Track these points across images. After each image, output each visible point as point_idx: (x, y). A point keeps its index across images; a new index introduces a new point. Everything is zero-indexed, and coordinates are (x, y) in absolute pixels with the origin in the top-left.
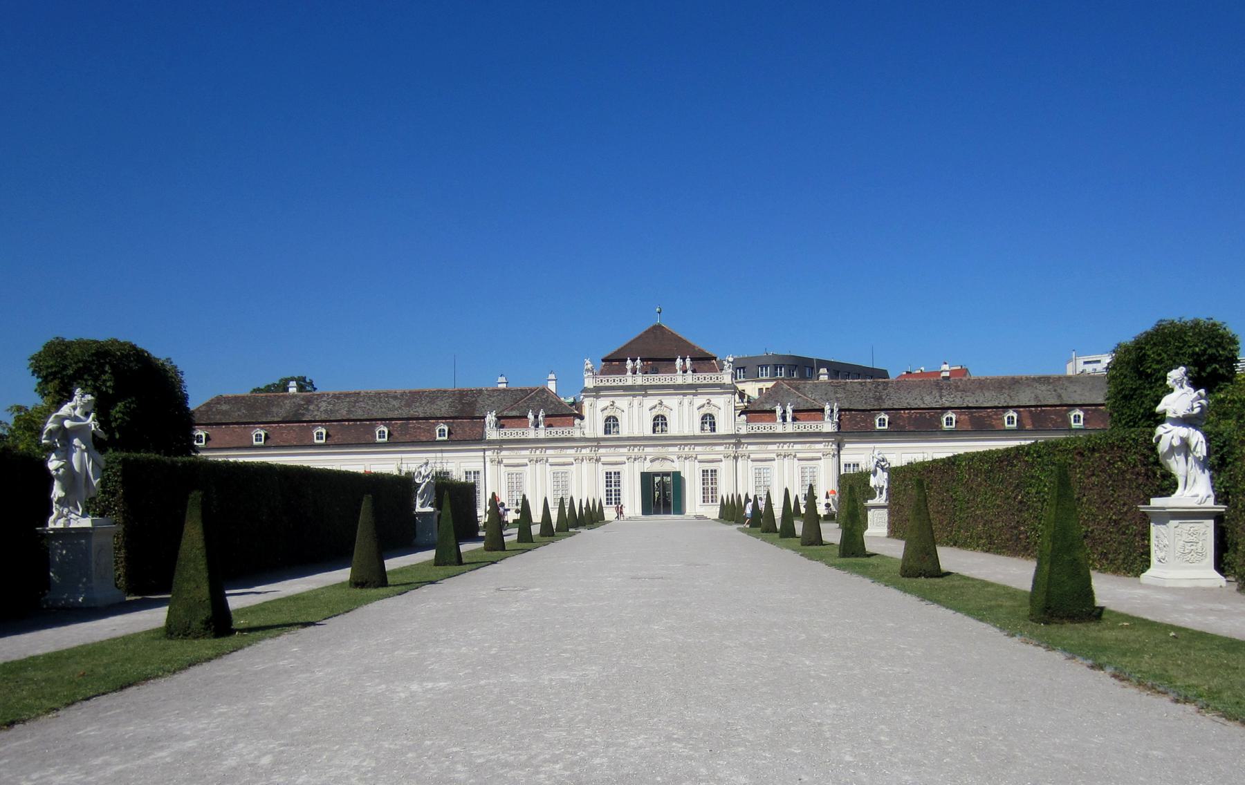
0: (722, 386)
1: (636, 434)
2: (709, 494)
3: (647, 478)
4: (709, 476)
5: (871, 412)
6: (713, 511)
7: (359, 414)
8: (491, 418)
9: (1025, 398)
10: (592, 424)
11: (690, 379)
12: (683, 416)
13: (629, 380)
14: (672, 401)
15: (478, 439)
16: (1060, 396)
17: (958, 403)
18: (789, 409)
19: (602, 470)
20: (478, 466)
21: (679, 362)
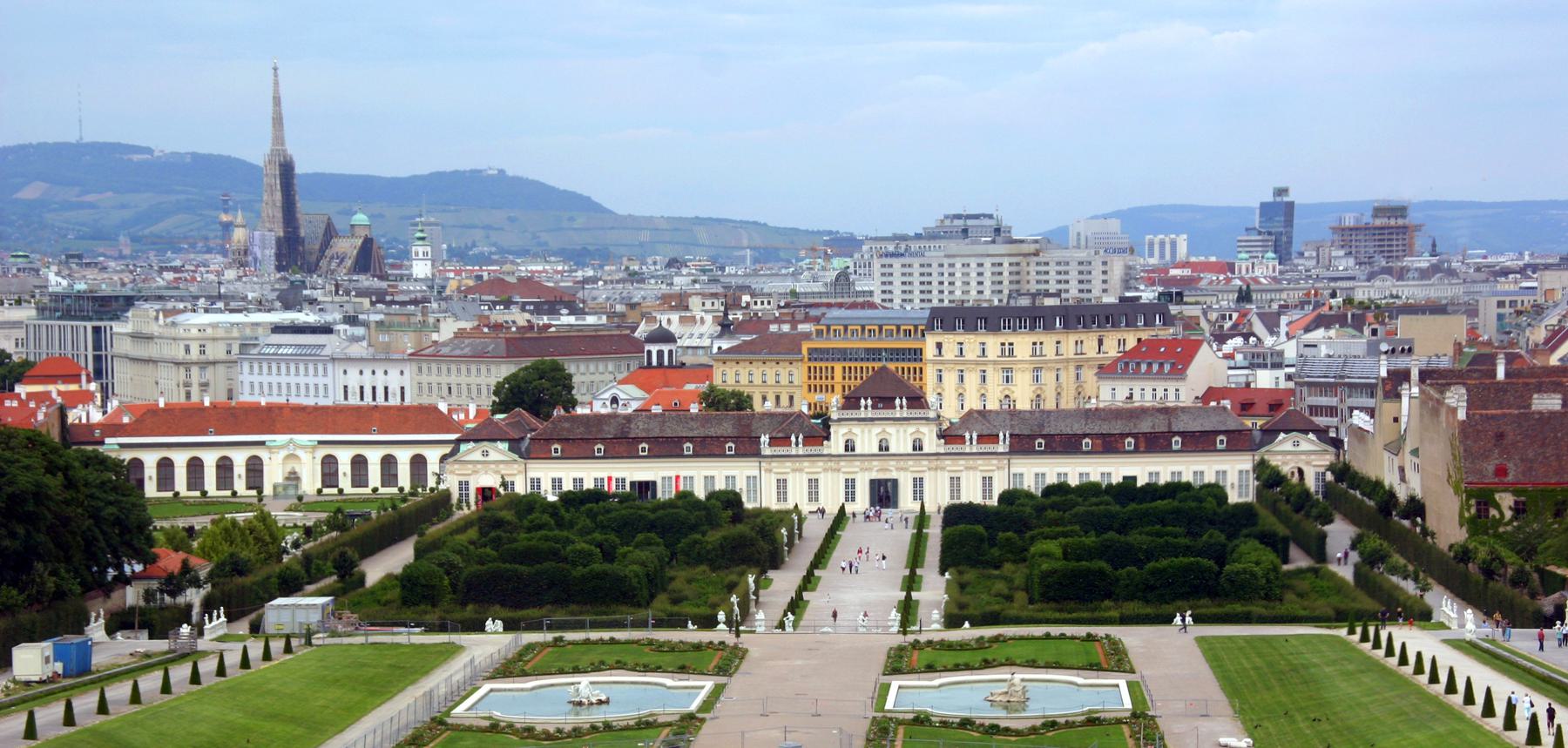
0: (927, 419)
1: (866, 452)
2: (918, 493)
3: (872, 482)
4: (918, 483)
5: (1033, 437)
7: (669, 433)
8: (765, 439)
9: (1145, 426)
10: (836, 445)
11: (905, 413)
12: (901, 440)
13: (862, 413)
14: (891, 429)
15: (756, 454)
16: (1170, 425)
17: (1096, 430)
18: (975, 436)
20: (756, 473)
21: (898, 401)
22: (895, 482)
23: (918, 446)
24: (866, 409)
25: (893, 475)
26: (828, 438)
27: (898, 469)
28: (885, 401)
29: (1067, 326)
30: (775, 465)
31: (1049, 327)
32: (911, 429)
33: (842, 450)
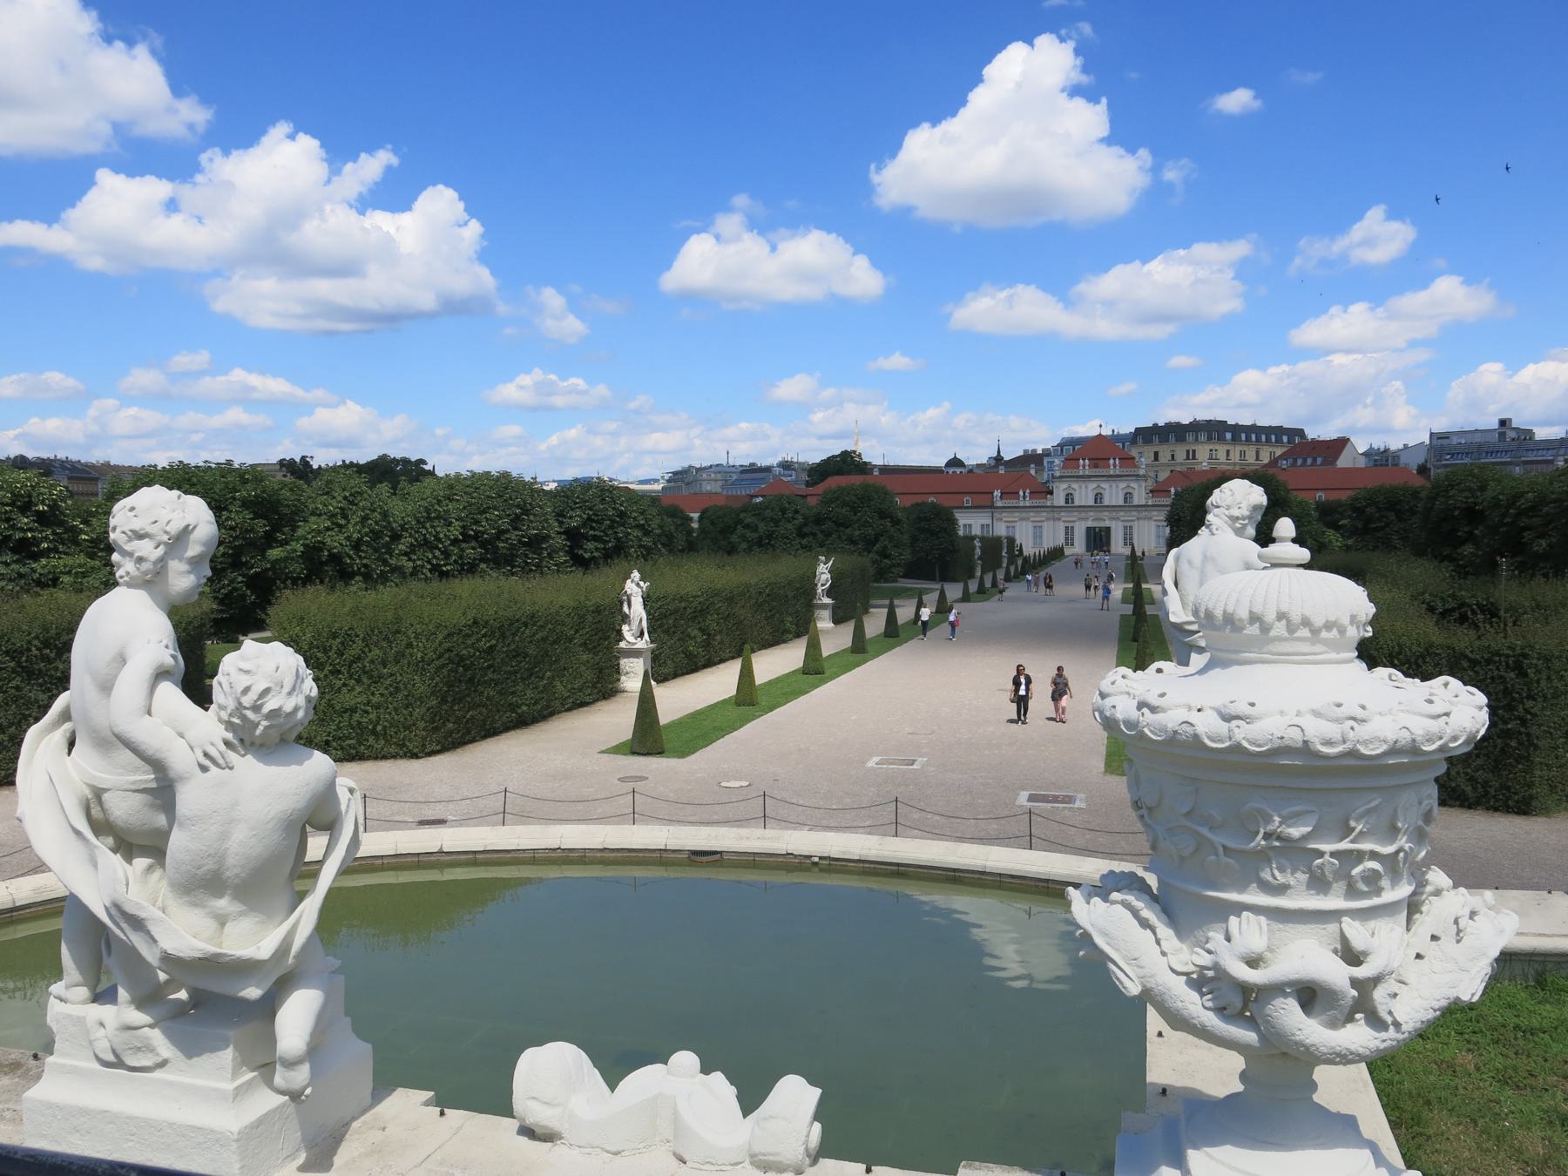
2: (1128, 540)
6: (1127, 551)
8: (997, 493)
10: (1059, 498)
12: (1113, 494)
19: (1061, 527)
22: (1108, 529)
23: (1128, 496)
24: (1084, 467)
25: (1107, 524)
26: (1051, 493)
27: (1111, 519)
28: (1098, 461)
29: (1236, 439)
30: (1006, 516)
31: (1221, 439)
32: (1122, 485)
33: (1062, 503)
